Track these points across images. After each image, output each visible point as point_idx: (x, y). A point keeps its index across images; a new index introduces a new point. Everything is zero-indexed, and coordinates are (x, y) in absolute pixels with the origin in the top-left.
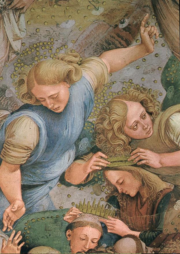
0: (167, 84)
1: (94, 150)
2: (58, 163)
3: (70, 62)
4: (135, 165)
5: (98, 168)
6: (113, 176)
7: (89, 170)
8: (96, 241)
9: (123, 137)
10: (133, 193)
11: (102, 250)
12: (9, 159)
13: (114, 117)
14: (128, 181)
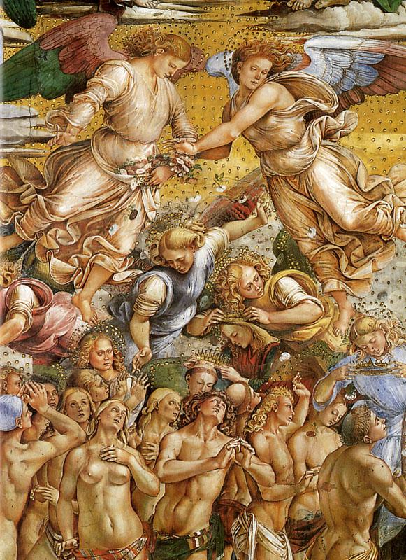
0: (277, 252)
1: (213, 307)
2: (181, 316)
3: (196, 231)
4: (248, 321)
5: (215, 322)
6: (228, 330)
7: (208, 324)
8: (211, 385)
9: (238, 296)
10: (244, 346)
11: (216, 393)
12: (140, 312)
13: (231, 279)
14: (240, 335)
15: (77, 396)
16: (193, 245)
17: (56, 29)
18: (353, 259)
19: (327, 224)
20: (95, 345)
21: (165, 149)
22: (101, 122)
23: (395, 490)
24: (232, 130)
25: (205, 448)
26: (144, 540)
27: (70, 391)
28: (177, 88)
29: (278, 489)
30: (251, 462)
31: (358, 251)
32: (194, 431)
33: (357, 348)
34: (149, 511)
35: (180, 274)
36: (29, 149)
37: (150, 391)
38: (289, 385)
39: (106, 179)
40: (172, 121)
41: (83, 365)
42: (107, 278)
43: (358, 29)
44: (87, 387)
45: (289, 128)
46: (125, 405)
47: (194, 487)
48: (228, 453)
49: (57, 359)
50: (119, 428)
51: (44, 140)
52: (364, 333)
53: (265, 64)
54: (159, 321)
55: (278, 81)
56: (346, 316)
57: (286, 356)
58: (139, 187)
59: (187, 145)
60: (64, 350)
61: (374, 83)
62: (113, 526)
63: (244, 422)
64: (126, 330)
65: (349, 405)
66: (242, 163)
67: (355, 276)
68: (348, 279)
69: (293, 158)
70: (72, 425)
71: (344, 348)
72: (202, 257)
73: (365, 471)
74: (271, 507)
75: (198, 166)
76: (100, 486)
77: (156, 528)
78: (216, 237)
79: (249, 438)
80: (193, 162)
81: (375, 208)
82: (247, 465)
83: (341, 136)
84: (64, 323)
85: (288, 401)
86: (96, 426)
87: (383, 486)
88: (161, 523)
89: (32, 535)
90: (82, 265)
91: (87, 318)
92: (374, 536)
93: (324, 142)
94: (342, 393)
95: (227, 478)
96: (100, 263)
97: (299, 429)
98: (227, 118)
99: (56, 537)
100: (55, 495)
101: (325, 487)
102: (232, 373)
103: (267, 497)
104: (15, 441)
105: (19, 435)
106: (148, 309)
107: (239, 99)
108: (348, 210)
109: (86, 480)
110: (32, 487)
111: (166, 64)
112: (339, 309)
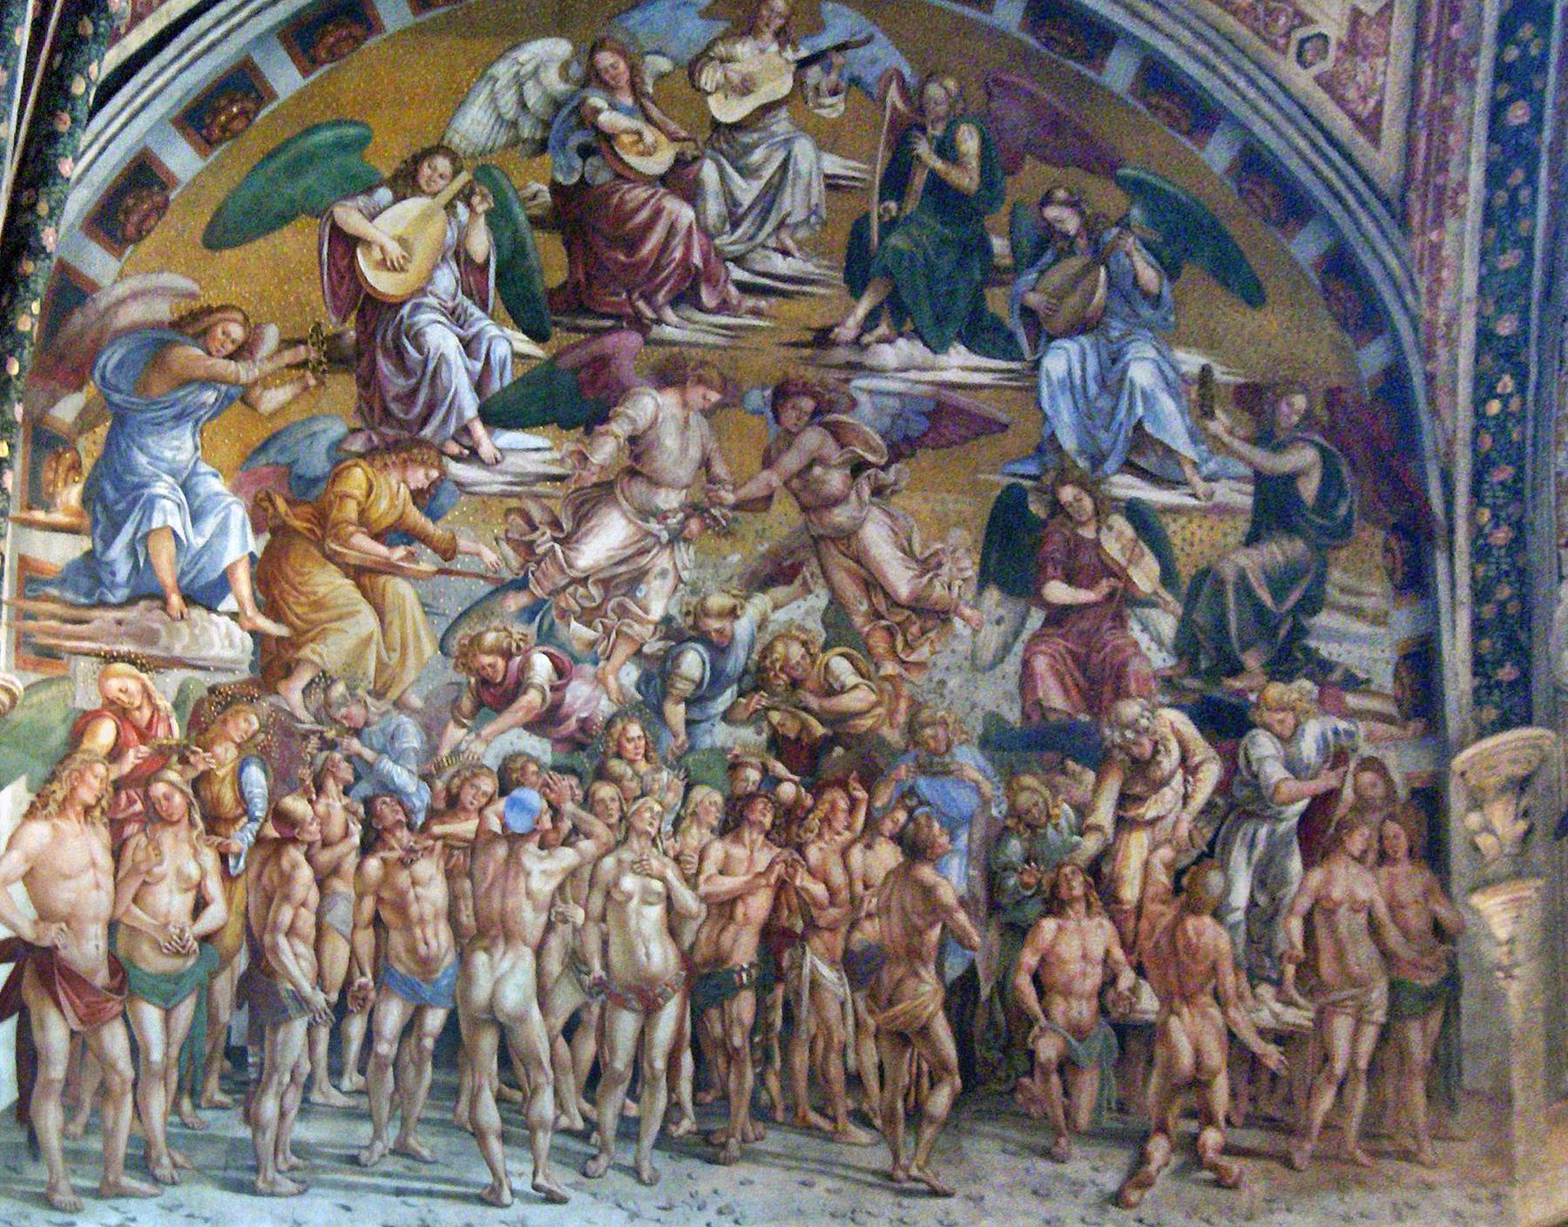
0: (827, 625)
1: (756, 689)
3: (734, 596)
6: (775, 717)
9: (784, 676)
10: (792, 735)
12: (675, 692)
13: (776, 655)
14: (789, 723)
15: (606, 791)
16: (733, 613)
17: (573, 347)
18: (909, 637)
19: (881, 596)
20: (624, 728)
21: (699, 497)
22: (626, 462)
23: (962, 917)
24: (773, 478)
25: (751, 860)
26: (683, 973)
27: (597, 785)
28: (711, 426)
29: (834, 912)
30: (802, 880)
31: (915, 629)
32: (738, 840)
33: (916, 744)
34: (688, 939)
35: (718, 648)
36: (539, 488)
37: (689, 788)
38: (843, 784)
39: (631, 529)
40: (706, 463)
41: (610, 752)
42: (635, 648)
43: (906, 370)
44: (617, 780)
45: (835, 480)
46: (660, 803)
47: (740, 910)
48: (778, 868)
49: (581, 746)
50: (653, 831)
51: (561, 478)
52: (923, 726)
53: (807, 404)
54: (696, 701)
55: (820, 424)
56: (903, 705)
57: (839, 751)
58: (671, 542)
59: (722, 493)
60: (591, 736)
61: (925, 434)
62: (648, 955)
63: (794, 828)
64: (659, 712)
65: (911, 811)
66: (784, 518)
67: (913, 658)
68: (903, 662)
69: (841, 516)
70: (599, 827)
71: (903, 744)
72: (743, 628)
73: (928, 892)
74: (827, 935)
75: (735, 520)
76: (634, 903)
77: (698, 958)
78: (759, 604)
79: (800, 849)
80: (730, 515)
81: (931, 580)
82: (798, 882)
83: (894, 492)
84: (587, 702)
85: (843, 804)
86: (628, 830)
87: (948, 910)
88: (703, 951)
89: (554, 965)
90: (607, 631)
91: (614, 697)
92: (940, 973)
93: (875, 500)
94: (903, 796)
95: (777, 898)
96: (629, 631)
97: (853, 842)
98: (768, 462)
99: (584, 968)
100: (579, 915)
101: (884, 910)
102: (780, 769)
103: (822, 923)
104: (532, 846)
105: (537, 838)
106: (683, 687)
107: (781, 444)
108: (902, 580)
109: (618, 896)
110: (552, 904)
111: (696, 395)
112: (897, 697)
